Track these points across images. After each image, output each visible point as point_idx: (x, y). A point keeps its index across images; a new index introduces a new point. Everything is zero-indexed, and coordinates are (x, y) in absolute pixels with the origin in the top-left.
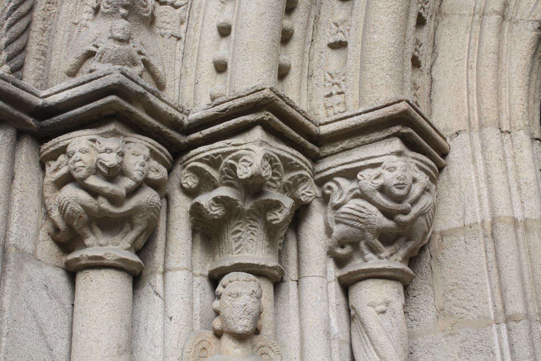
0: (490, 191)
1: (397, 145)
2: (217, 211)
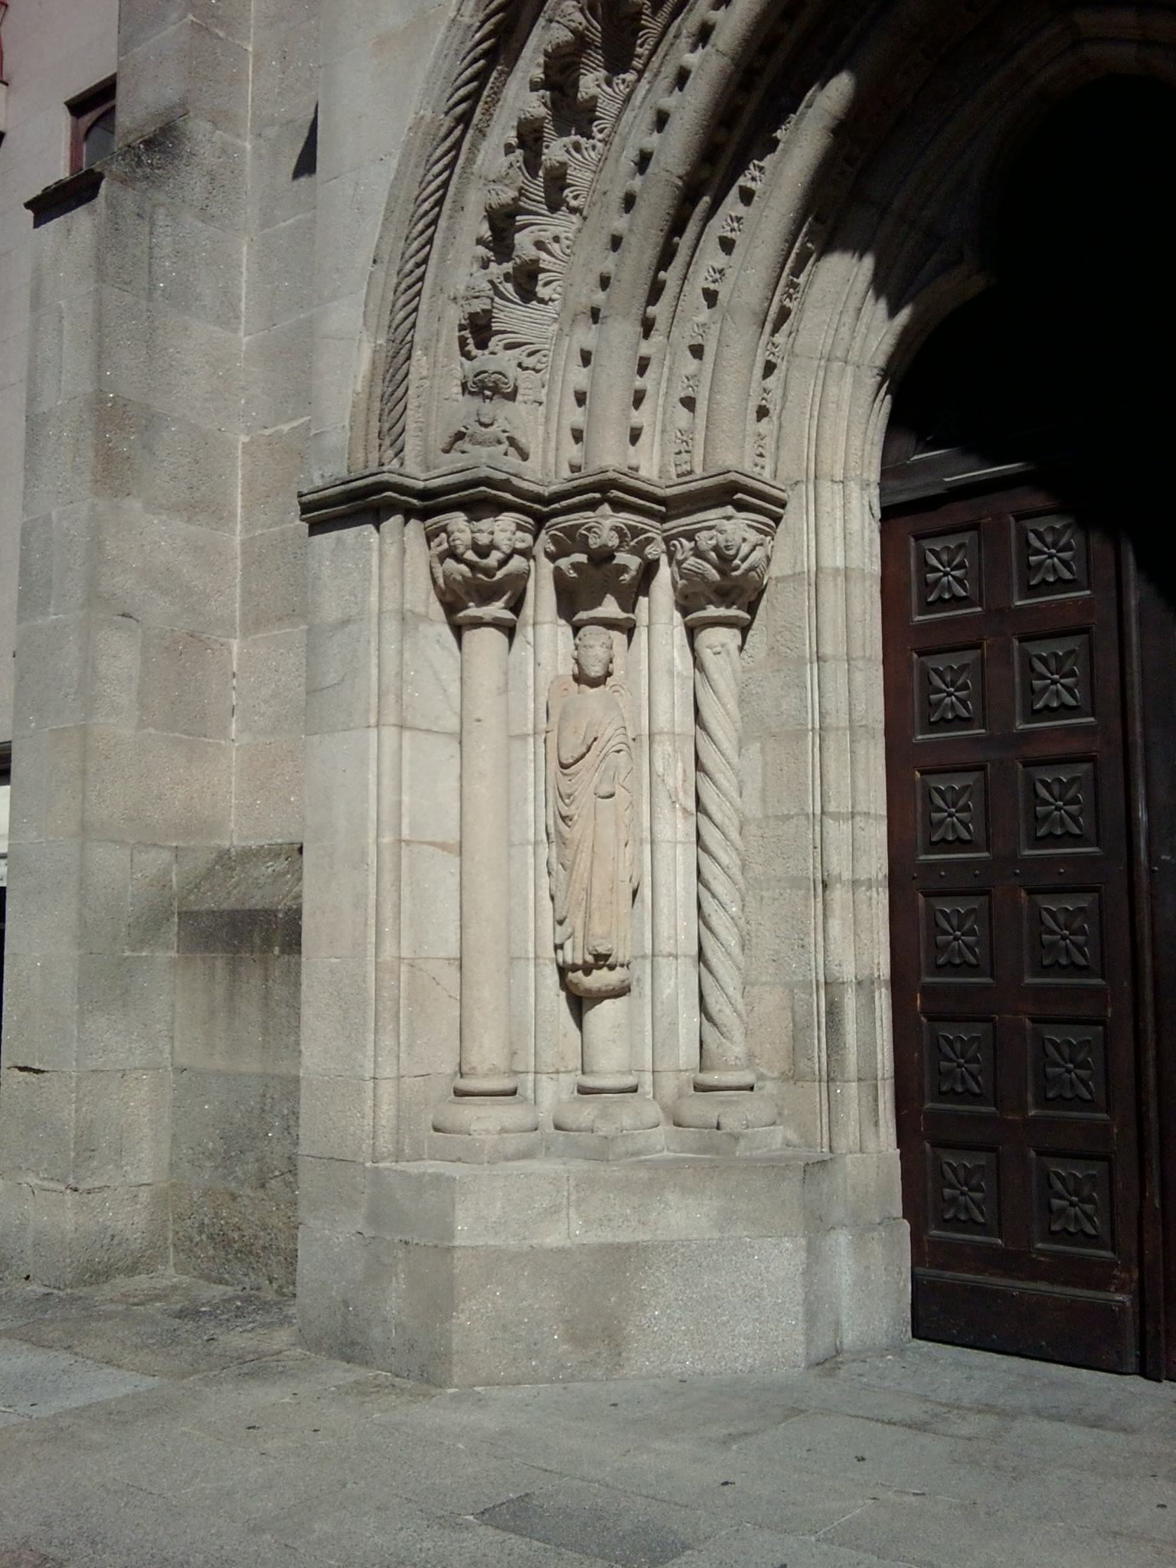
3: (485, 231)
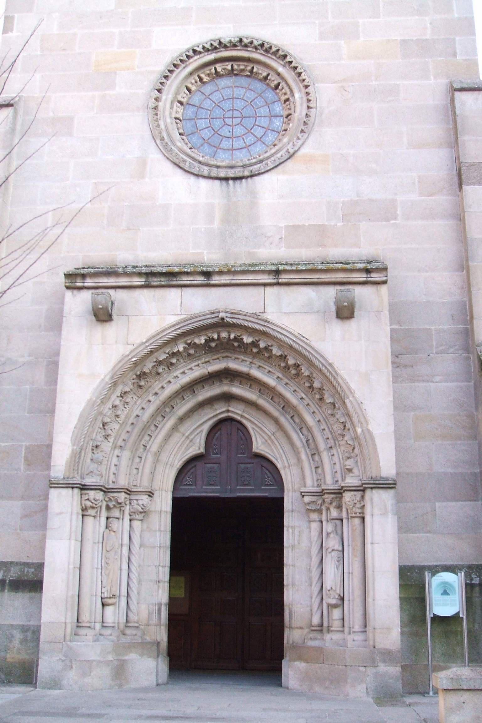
0: (161, 505)
1: (147, 496)
2: (112, 507)
3: (101, 426)
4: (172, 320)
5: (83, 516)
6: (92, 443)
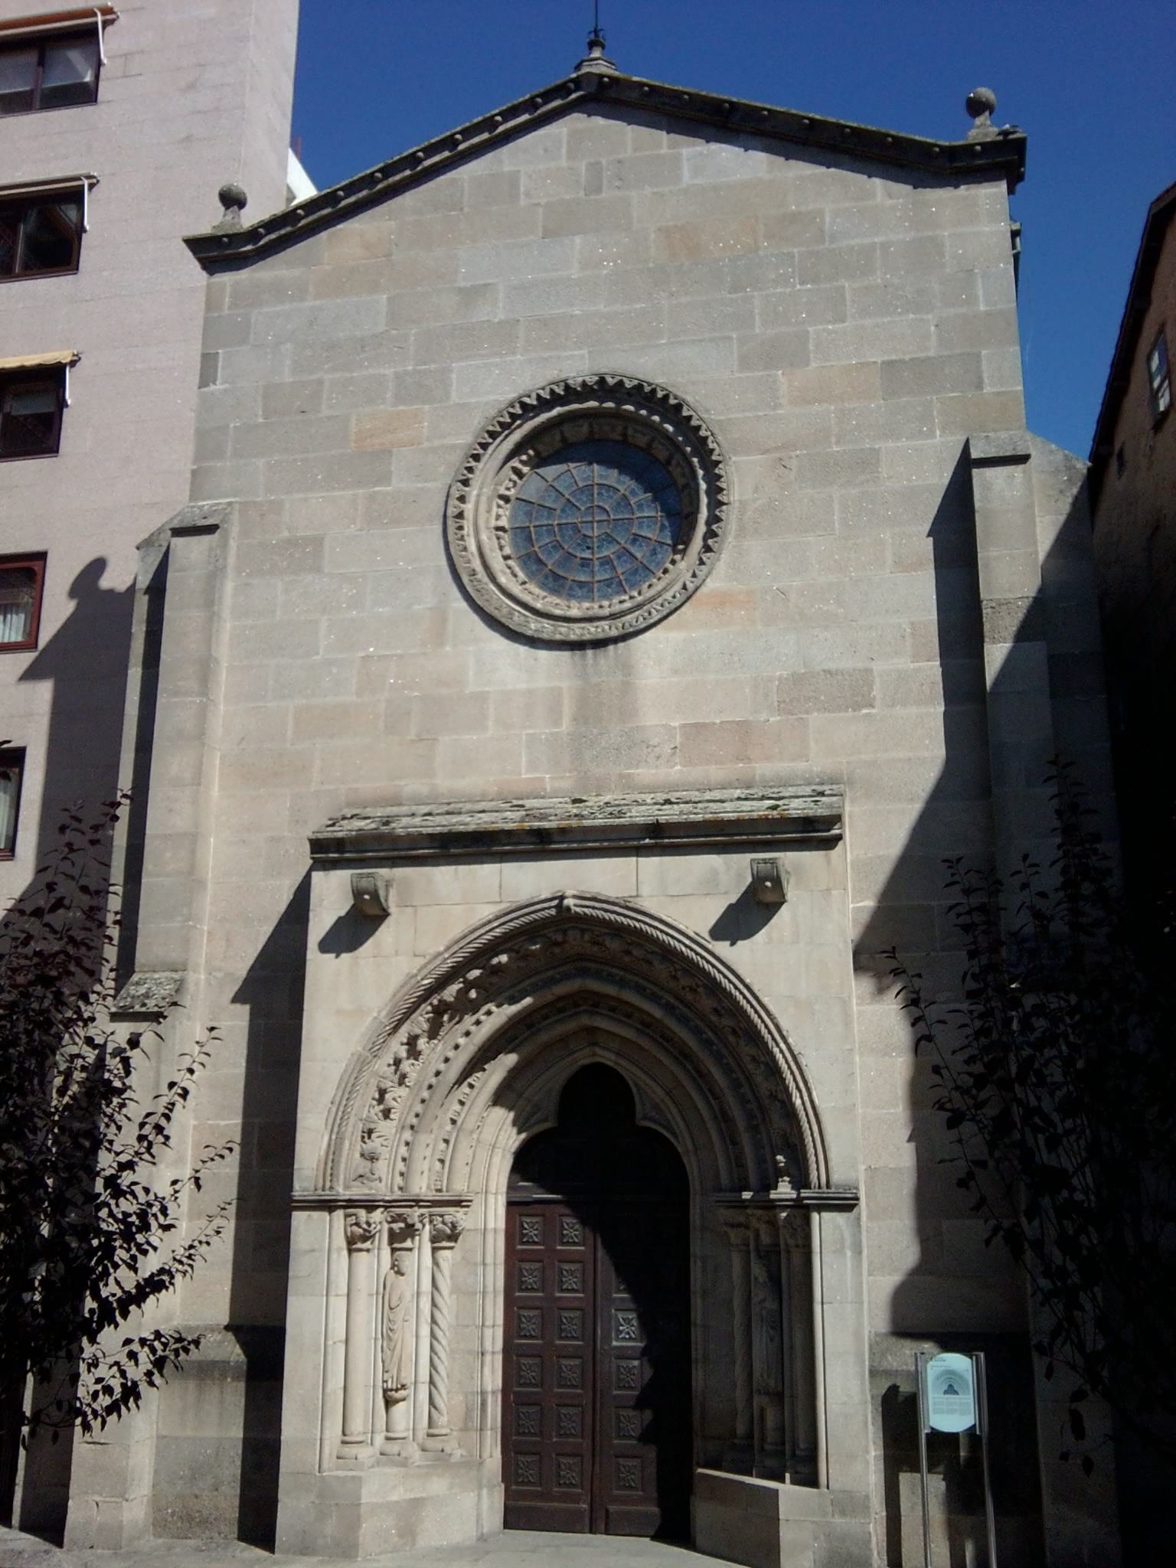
3: (377, 1096)
4: (487, 912)
5: (350, 1251)
6: (361, 1126)
